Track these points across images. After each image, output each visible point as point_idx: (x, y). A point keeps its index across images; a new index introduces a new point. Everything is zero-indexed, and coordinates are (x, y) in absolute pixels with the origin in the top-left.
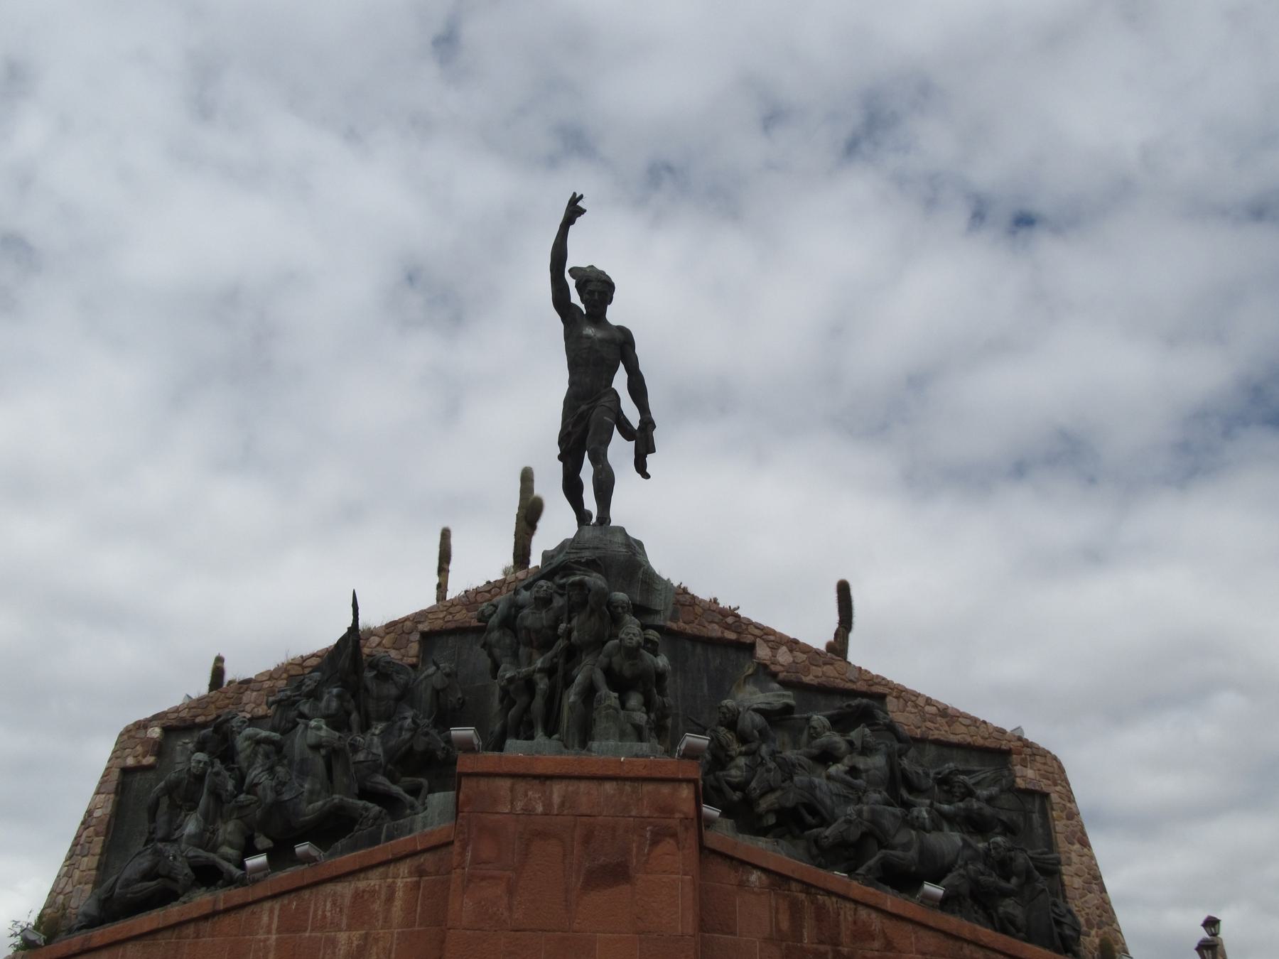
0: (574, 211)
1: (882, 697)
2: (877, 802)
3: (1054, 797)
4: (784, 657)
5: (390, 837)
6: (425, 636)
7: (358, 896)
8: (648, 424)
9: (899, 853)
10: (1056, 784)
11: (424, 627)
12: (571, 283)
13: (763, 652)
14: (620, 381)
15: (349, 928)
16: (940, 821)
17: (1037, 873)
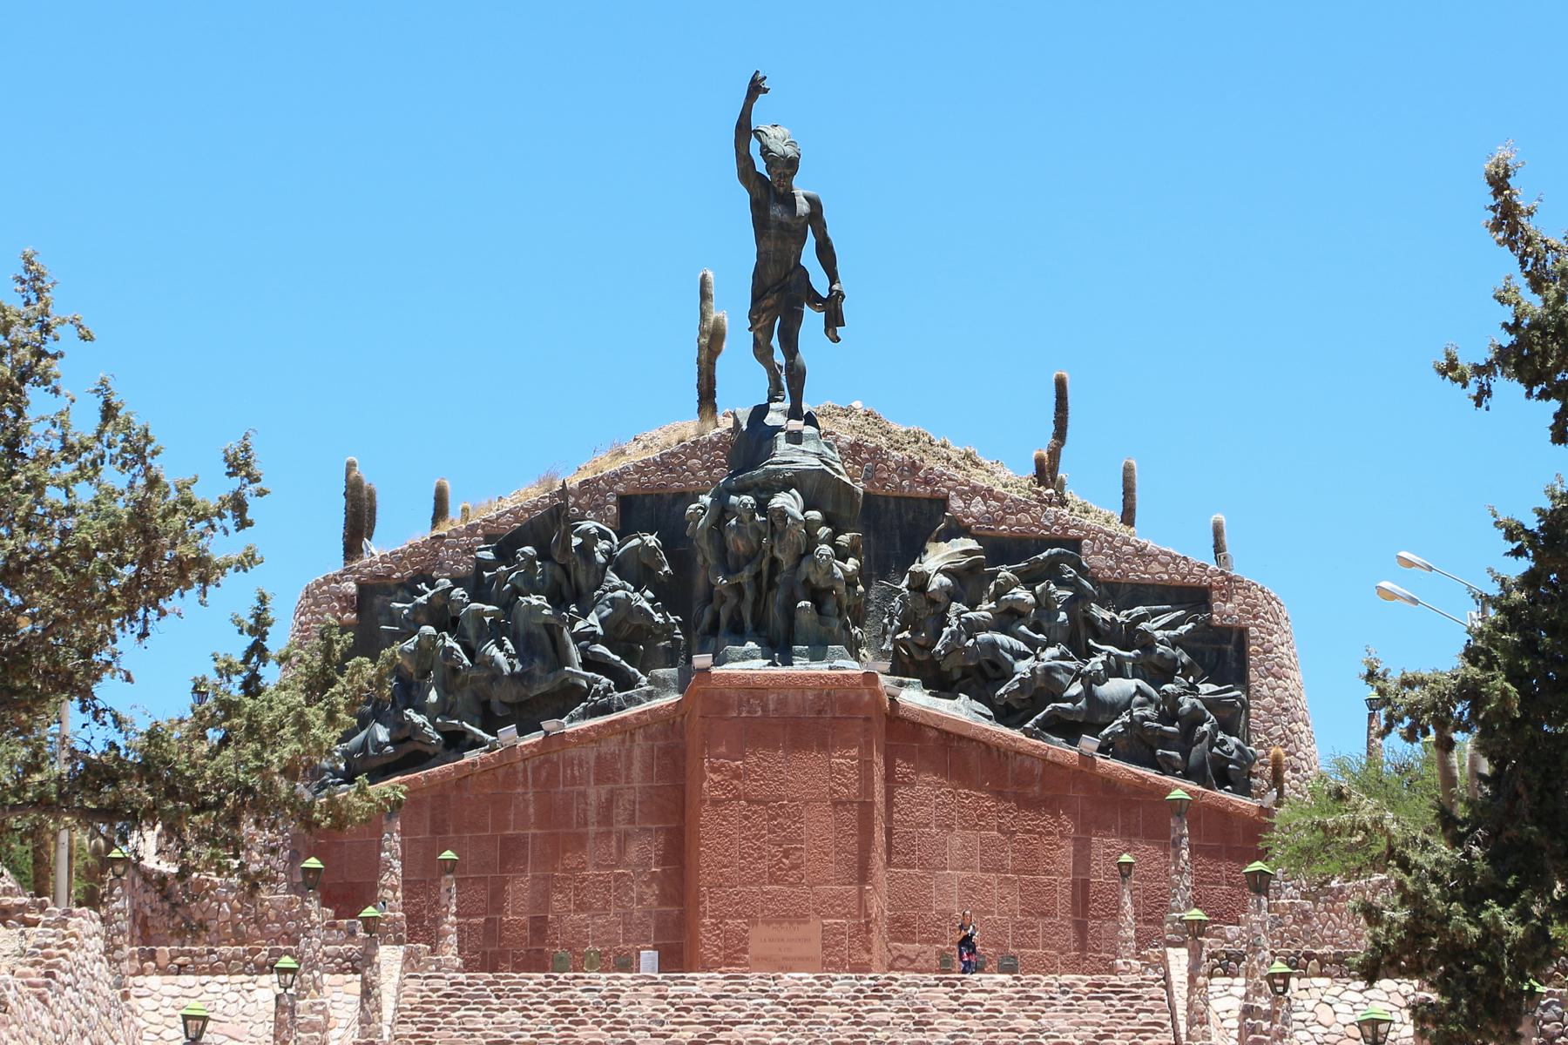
0: (756, 88)
1: (1075, 544)
2: (1054, 658)
3: (1254, 631)
4: (977, 506)
5: (621, 709)
6: (625, 502)
7: (598, 757)
9: (1068, 705)
10: (1256, 617)
11: (620, 488)
13: (956, 504)
14: (809, 257)
15: (598, 781)
16: (1115, 669)
17: (1208, 714)
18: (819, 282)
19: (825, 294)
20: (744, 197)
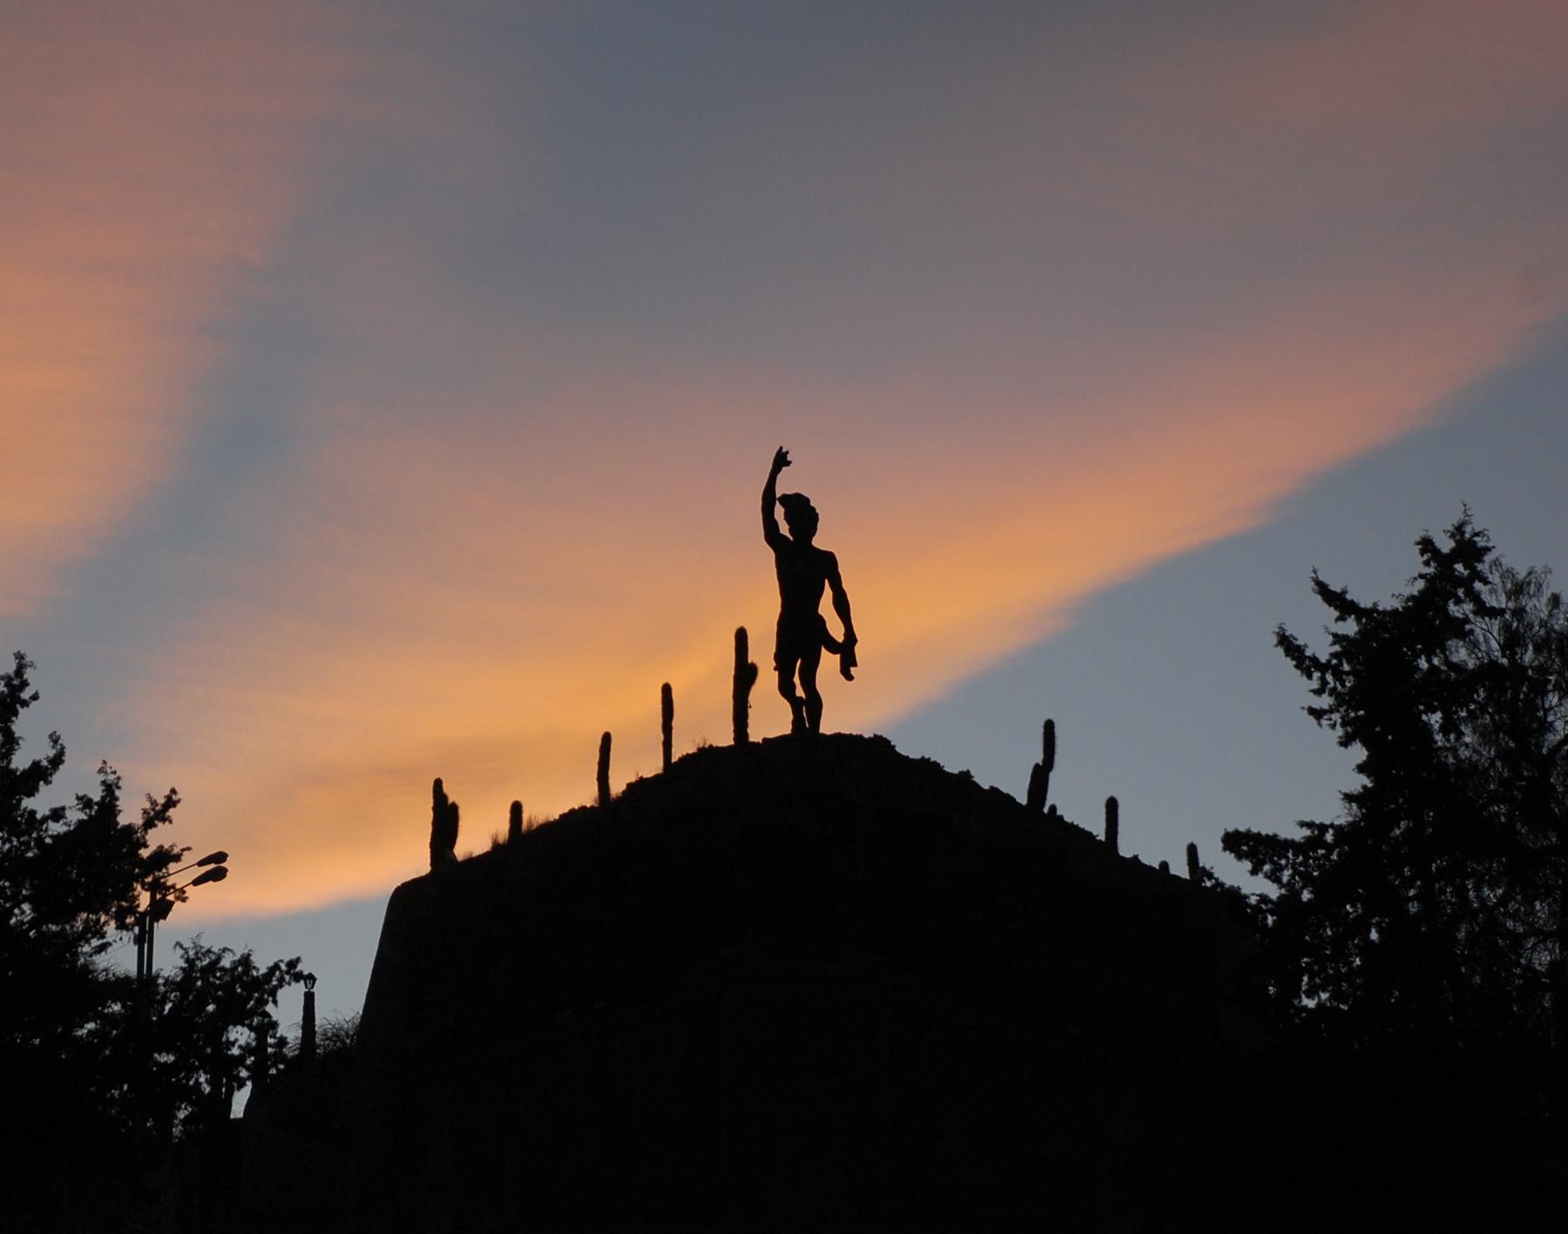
0: (781, 460)
8: (851, 637)
12: (779, 512)
18: (836, 630)
19: (840, 638)
20: (770, 555)
